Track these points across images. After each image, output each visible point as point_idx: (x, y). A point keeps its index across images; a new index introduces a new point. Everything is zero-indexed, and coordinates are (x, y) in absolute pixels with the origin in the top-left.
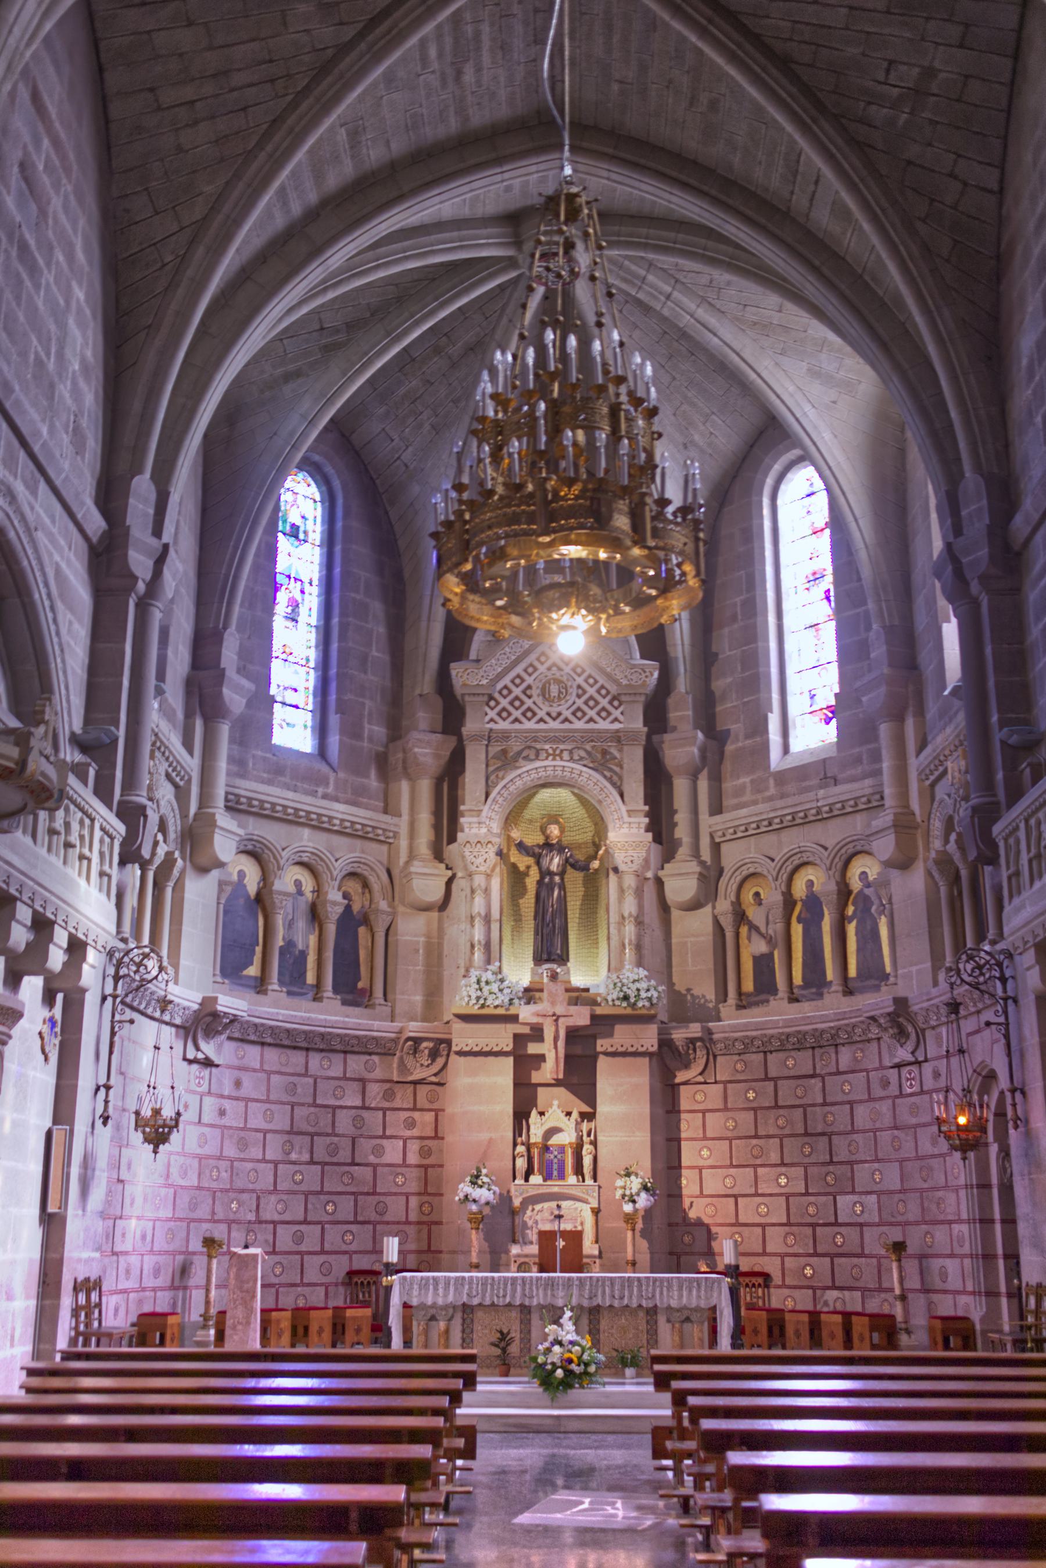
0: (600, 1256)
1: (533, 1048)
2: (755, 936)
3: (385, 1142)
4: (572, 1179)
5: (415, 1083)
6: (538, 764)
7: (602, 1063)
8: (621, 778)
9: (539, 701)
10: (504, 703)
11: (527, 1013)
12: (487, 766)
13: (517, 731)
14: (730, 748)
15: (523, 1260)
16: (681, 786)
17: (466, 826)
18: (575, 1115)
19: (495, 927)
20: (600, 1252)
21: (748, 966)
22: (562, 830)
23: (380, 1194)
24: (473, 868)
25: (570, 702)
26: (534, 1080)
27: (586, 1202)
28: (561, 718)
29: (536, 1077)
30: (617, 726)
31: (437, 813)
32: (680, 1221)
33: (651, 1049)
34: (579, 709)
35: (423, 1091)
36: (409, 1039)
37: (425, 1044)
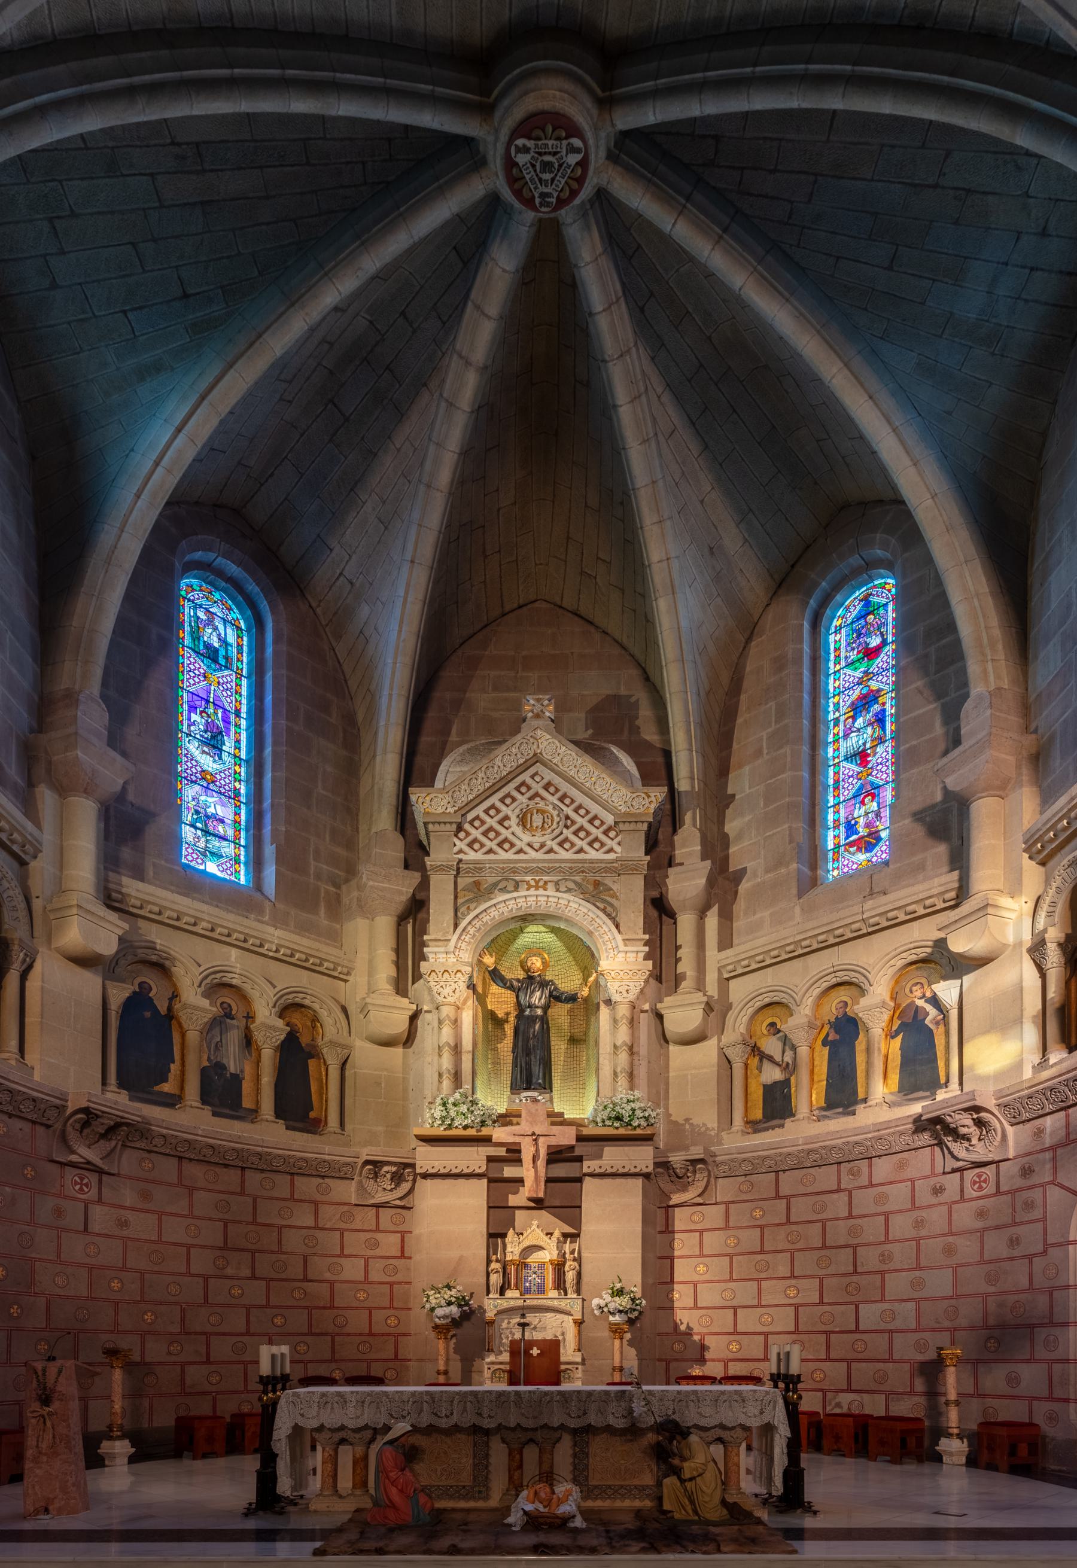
1: (509, 1171)
2: (766, 1064)
3: (343, 1261)
4: (554, 1293)
5: (377, 1206)
6: (515, 894)
9: (518, 830)
10: (476, 833)
12: (456, 897)
13: (490, 862)
14: (744, 886)
16: (686, 922)
17: (431, 956)
18: (557, 1234)
20: (583, 1359)
21: (757, 1094)
22: (545, 963)
23: (338, 1308)
24: (440, 999)
25: (557, 832)
27: (569, 1314)
28: (545, 849)
29: (513, 1200)
30: (612, 856)
31: (399, 950)
32: (671, 1330)
34: (566, 840)
35: (385, 1214)
36: (367, 1162)
37: (386, 1168)
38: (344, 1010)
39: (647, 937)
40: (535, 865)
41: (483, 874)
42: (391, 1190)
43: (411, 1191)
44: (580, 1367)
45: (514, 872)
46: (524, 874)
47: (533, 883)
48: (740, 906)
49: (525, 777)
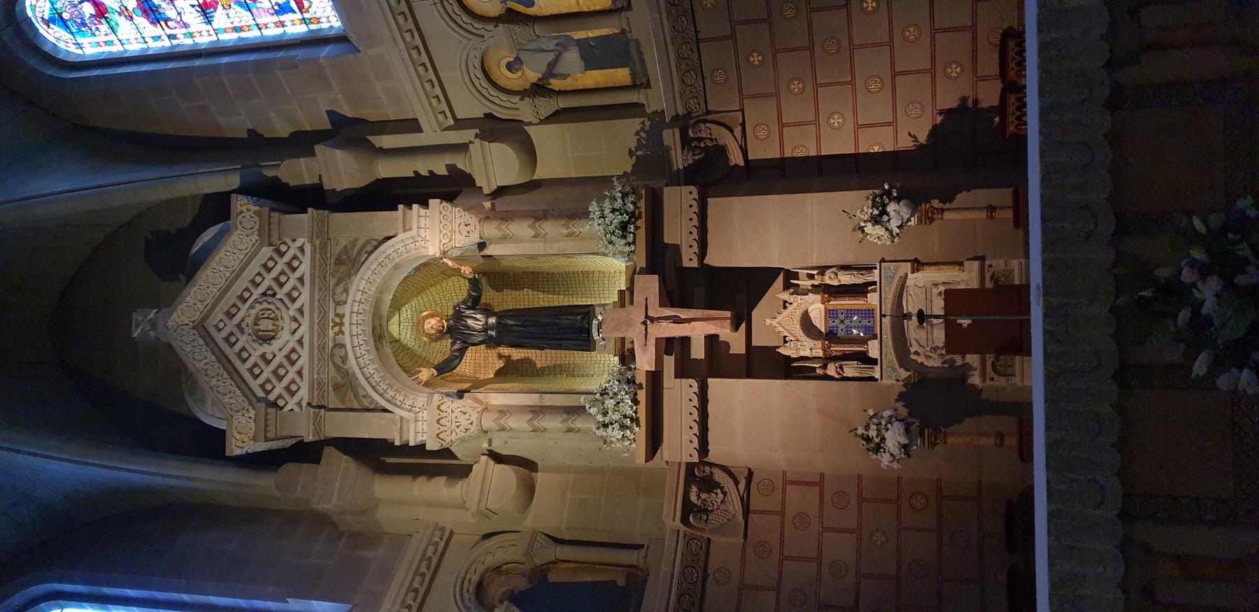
0: (982, 259)
1: (698, 351)
2: (560, 69)
4: (873, 299)
6: (349, 347)
7: (715, 259)
8: (368, 242)
9: (276, 344)
10: (279, 389)
11: (645, 362)
12: (352, 410)
13: (311, 372)
15: (989, 368)
17: (420, 439)
18: (785, 296)
19: (549, 400)
20: (975, 258)
24: (473, 428)
25: (279, 304)
26: (743, 351)
28: (298, 316)
30: (308, 248)
33: (695, 195)
35: (756, 502)
36: (685, 520)
37: (693, 498)
38: (488, 536)
39: (401, 207)
40: (316, 327)
41: (325, 381)
42: (725, 494)
43: (724, 469)
44: (987, 263)
45: (324, 348)
46: (326, 338)
47: (337, 329)
48: (371, 115)
49: (219, 337)
